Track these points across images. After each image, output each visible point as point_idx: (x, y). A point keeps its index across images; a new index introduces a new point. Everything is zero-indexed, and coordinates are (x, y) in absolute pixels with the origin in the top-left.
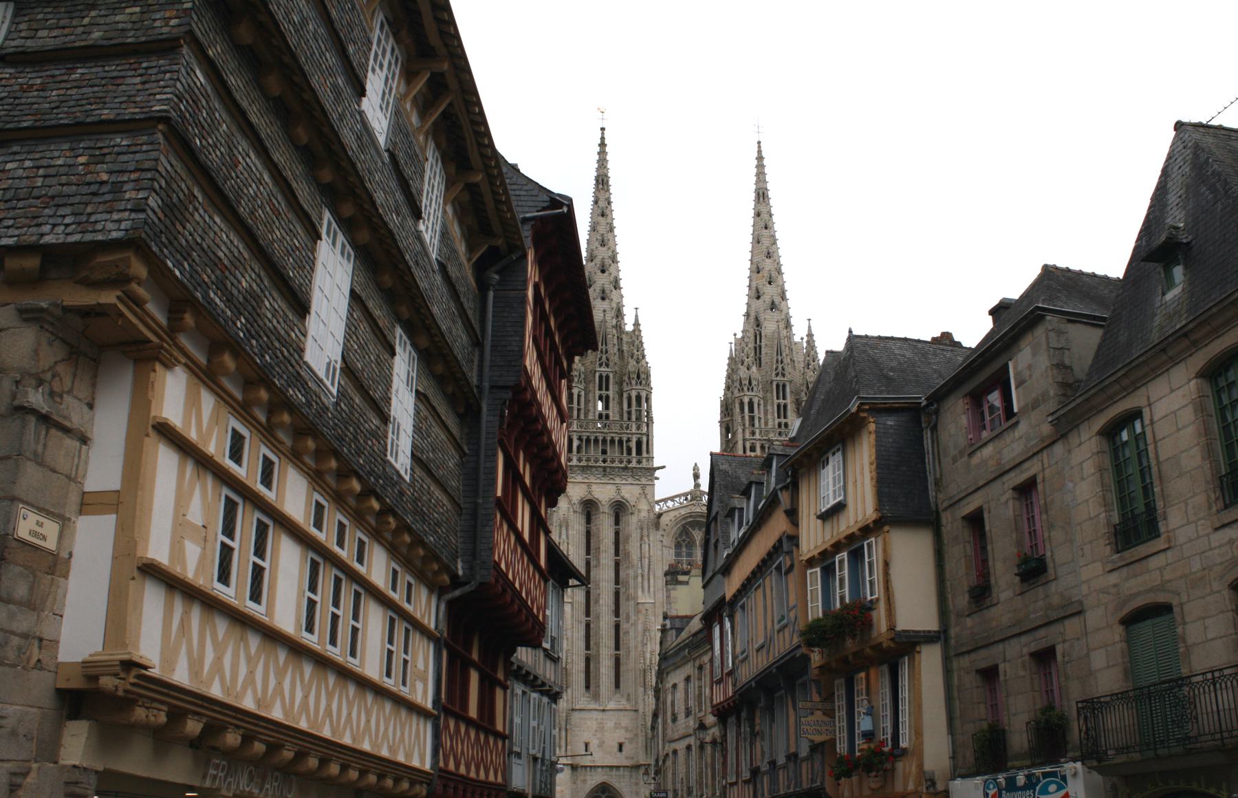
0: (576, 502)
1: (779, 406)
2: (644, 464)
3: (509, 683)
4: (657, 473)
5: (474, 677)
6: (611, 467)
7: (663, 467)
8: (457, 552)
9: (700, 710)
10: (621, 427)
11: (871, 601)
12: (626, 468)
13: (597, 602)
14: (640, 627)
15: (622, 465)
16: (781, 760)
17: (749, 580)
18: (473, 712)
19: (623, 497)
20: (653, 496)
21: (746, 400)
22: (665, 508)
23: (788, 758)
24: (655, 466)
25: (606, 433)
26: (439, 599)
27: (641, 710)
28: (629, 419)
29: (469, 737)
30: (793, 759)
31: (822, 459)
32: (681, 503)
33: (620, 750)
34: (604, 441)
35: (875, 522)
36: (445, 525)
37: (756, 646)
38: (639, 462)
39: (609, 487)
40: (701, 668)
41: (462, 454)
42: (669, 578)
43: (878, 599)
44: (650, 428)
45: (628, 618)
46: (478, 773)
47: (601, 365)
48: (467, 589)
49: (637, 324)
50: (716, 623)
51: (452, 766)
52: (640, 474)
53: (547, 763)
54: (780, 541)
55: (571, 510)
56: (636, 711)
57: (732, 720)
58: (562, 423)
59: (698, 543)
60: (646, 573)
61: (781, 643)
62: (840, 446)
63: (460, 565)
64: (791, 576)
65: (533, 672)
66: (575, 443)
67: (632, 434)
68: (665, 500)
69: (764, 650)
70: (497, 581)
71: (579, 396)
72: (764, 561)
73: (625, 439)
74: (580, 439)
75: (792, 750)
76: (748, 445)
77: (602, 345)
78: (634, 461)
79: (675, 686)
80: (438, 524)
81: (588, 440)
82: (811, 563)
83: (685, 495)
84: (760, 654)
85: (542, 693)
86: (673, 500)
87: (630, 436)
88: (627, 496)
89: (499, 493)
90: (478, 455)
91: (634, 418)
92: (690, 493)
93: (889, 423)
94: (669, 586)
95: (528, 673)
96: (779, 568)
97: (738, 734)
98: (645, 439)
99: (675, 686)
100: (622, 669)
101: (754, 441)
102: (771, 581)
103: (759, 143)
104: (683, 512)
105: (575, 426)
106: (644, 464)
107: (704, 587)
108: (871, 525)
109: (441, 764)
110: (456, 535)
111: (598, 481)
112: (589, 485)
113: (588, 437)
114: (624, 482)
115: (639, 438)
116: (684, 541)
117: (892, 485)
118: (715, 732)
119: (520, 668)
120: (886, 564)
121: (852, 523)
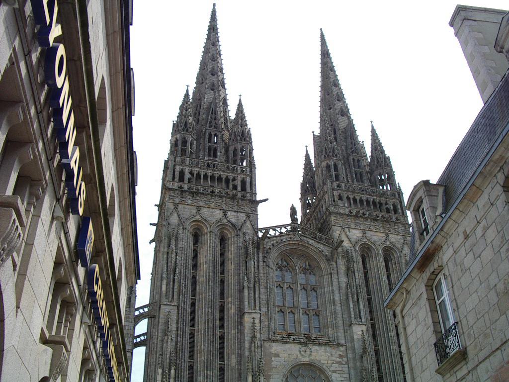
4: (261, 208)
21: (332, 163)
24: (258, 199)
34: (213, 177)
47: (210, 127)
49: (240, 105)
60: (252, 286)
66: (187, 176)
71: (192, 144)
74: (191, 173)
77: (212, 113)
81: (198, 175)
83: (285, 226)
86: (275, 230)
98: (248, 180)
112: (199, 208)
114: (230, 209)
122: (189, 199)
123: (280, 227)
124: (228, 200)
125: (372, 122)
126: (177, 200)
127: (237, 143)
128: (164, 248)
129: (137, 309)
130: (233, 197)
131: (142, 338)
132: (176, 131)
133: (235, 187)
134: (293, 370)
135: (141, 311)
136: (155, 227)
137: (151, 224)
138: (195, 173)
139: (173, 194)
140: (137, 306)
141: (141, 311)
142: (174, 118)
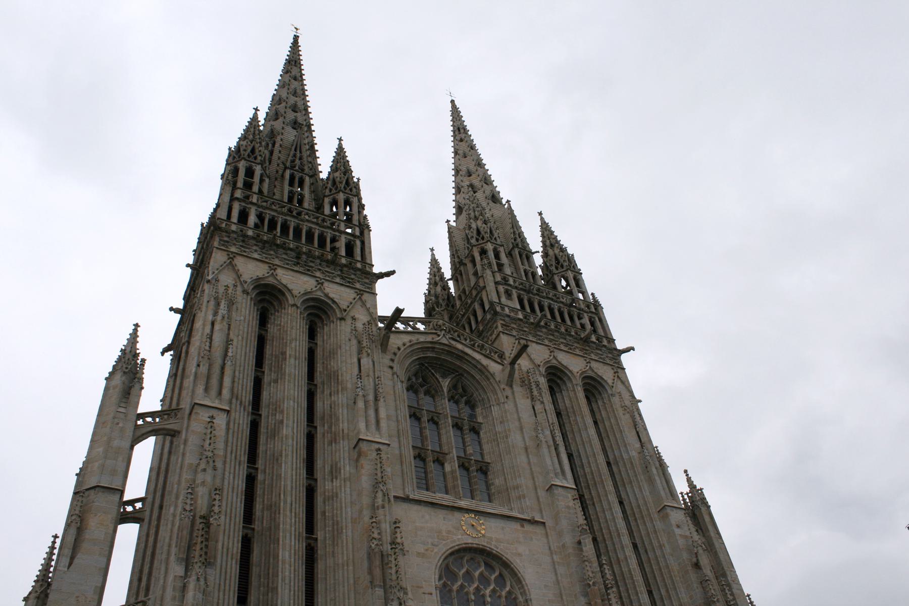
1: (526, 275)
7: (393, 272)
13: (274, 434)
14: (365, 482)
19: (327, 295)
24: (376, 270)
45: (335, 472)
52: (353, 276)
55: (239, 289)
59: (445, 390)
60: (371, 397)
66: (252, 219)
74: (260, 217)
76: (501, 289)
77: (296, 150)
98: (358, 243)
100: (320, 566)
101: (509, 288)
103: (452, 102)
113: (273, 217)
122: (256, 251)
125: (540, 214)
126: (233, 249)
127: (339, 192)
129: (143, 416)
130: (333, 263)
131: (139, 505)
132: (234, 158)
134: (451, 559)
135: (149, 419)
136: (179, 316)
137: (171, 309)
139: (226, 239)
140: (141, 410)
141: (149, 419)
142: (233, 144)
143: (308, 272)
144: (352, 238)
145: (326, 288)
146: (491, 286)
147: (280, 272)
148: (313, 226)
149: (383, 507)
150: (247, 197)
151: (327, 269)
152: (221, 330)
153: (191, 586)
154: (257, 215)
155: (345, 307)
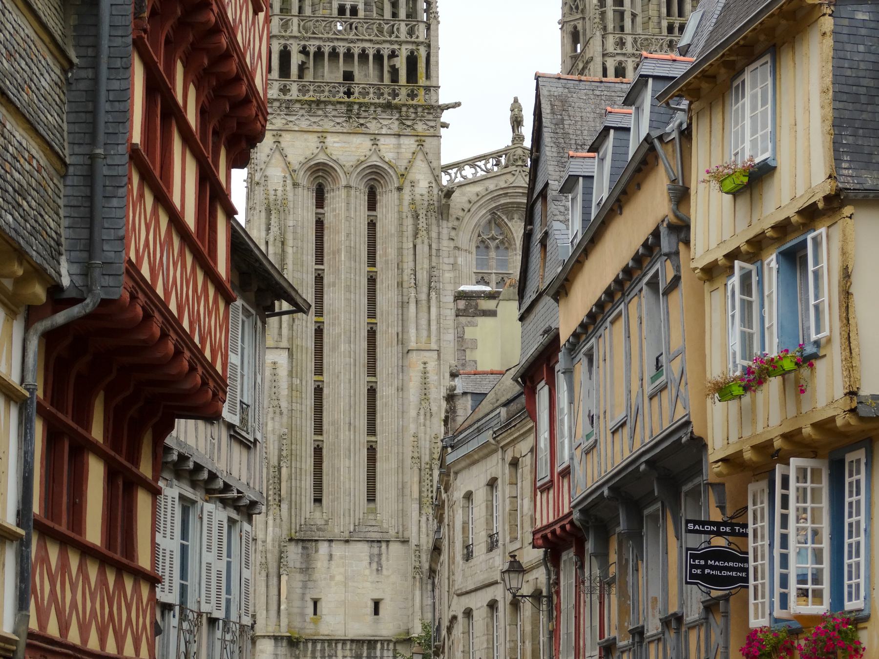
0: (297, 167)
2: (420, 100)
3: (161, 484)
4: (446, 116)
5: (96, 471)
6: (361, 105)
7: (457, 105)
8: (59, 244)
9: (514, 539)
10: (381, 31)
11: (817, 343)
12: (388, 106)
13: (334, 348)
15: (381, 101)
16: (653, 627)
17: (600, 305)
18: (94, 534)
20: (439, 159)
22: (459, 179)
23: (666, 622)
24: (442, 101)
25: (352, 42)
26: (27, 329)
27: (414, 541)
28: (395, 15)
29: (86, 579)
30: (674, 624)
31: (735, 84)
32: (487, 171)
33: (376, 612)
34: (349, 55)
35: (827, 199)
36: (34, 193)
37: (611, 424)
38: (412, 95)
39: (357, 140)
40: (515, 463)
41: (67, 65)
42: (462, 304)
43: (829, 340)
44: (432, 33)
46: (103, 641)
48: (76, 311)
50: (543, 383)
51: (53, 630)
53: (234, 627)
54: (656, 234)
55: (289, 182)
56: (405, 542)
57: (568, 556)
58: (256, 13)
60: (423, 297)
61: (656, 417)
62: (767, 58)
63: (64, 268)
64: (674, 296)
65: (209, 466)
66: (296, 59)
67: (400, 43)
68: (459, 165)
69: (626, 430)
70: (133, 297)
72: (627, 271)
73: (386, 53)
74: (304, 51)
75: (673, 609)
76: (611, 64)
78: (404, 92)
79: (469, 496)
80: (21, 192)
81: (319, 54)
82: (711, 272)
83: (497, 155)
84: (618, 436)
85: (225, 502)
86: (473, 166)
87: (396, 47)
88: (389, 156)
89: (137, 138)
90: (95, 66)
91: (402, 13)
92: (506, 151)
93: (860, 16)
94: (463, 320)
95: (198, 468)
96: (653, 284)
97: (580, 582)
98: (422, 52)
99: (469, 496)
102: (640, 305)
104: (491, 185)
105: (295, 28)
106: (420, 100)
107: (522, 319)
108: (821, 205)
109: (33, 625)
110: (58, 214)
111: (338, 128)
112: (322, 135)
114: (384, 131)
115: (412, 52)
116: (493, 239)
117: (861, 131)
118: (540, 577)
119: (183, 458)
120: (846, 274)
121: (785, 201)
123: (485, 157)
124: (379, 109)
128: (259, 230)
133: (394, 72)
138: (312, 50)
143: (360, 131)
144: (414, 48)
145: (381, 147)
146: (598, 60)
147: (332, 141)
148: (366, 45)
149: (424, 425)
150: (285, 26)
151: (384, 116)
152: (275, 254)
153: (271, 522)
154: (300, 52)
155: (403, 171)
